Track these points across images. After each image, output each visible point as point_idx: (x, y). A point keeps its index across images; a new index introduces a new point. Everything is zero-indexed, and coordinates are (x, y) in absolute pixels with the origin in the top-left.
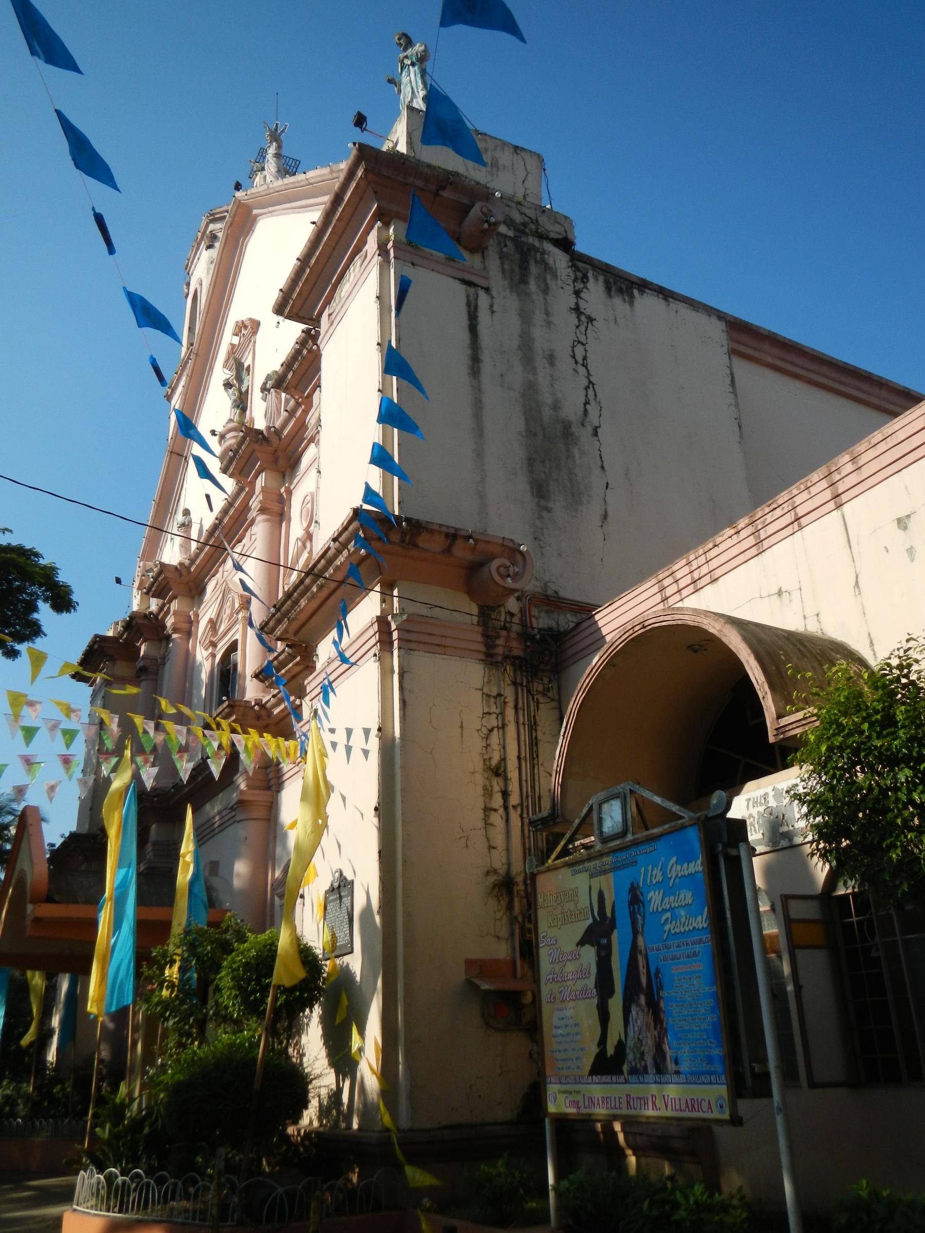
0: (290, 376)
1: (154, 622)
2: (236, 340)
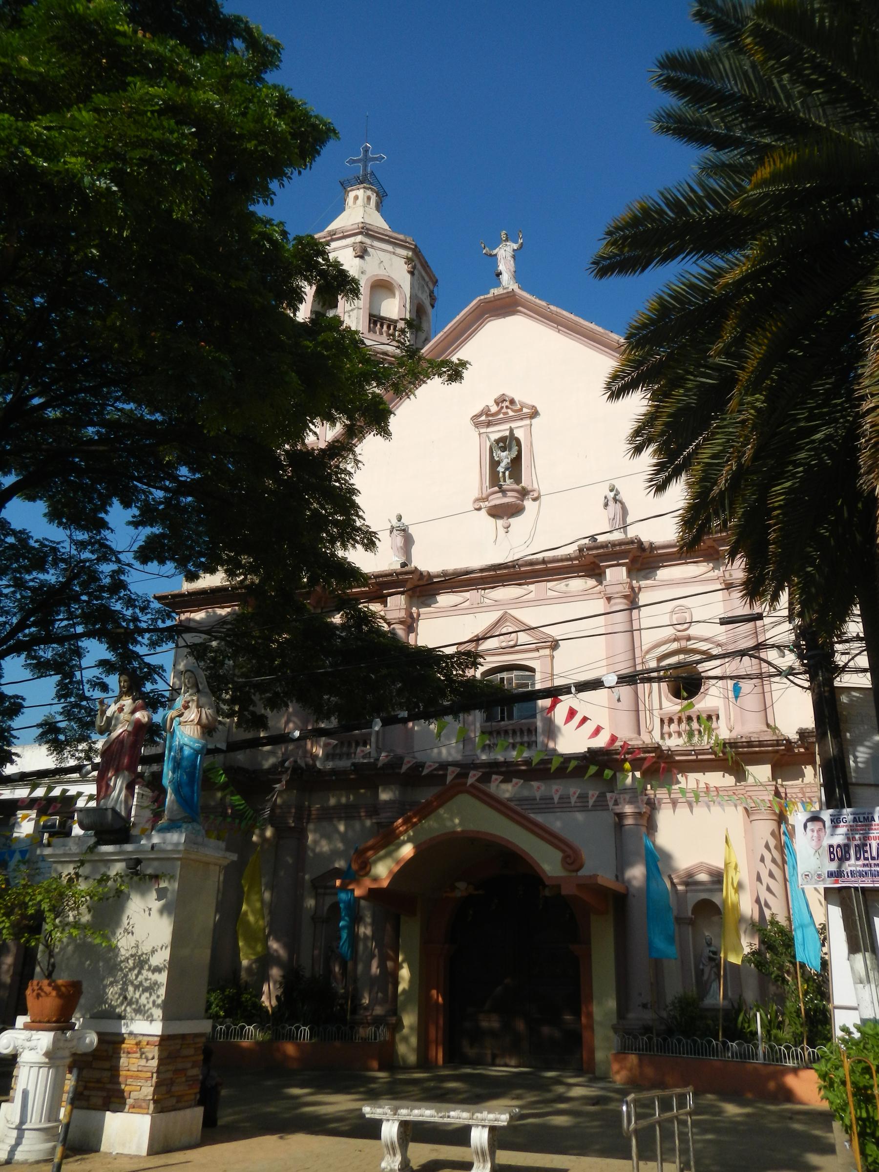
2: (494, 409)
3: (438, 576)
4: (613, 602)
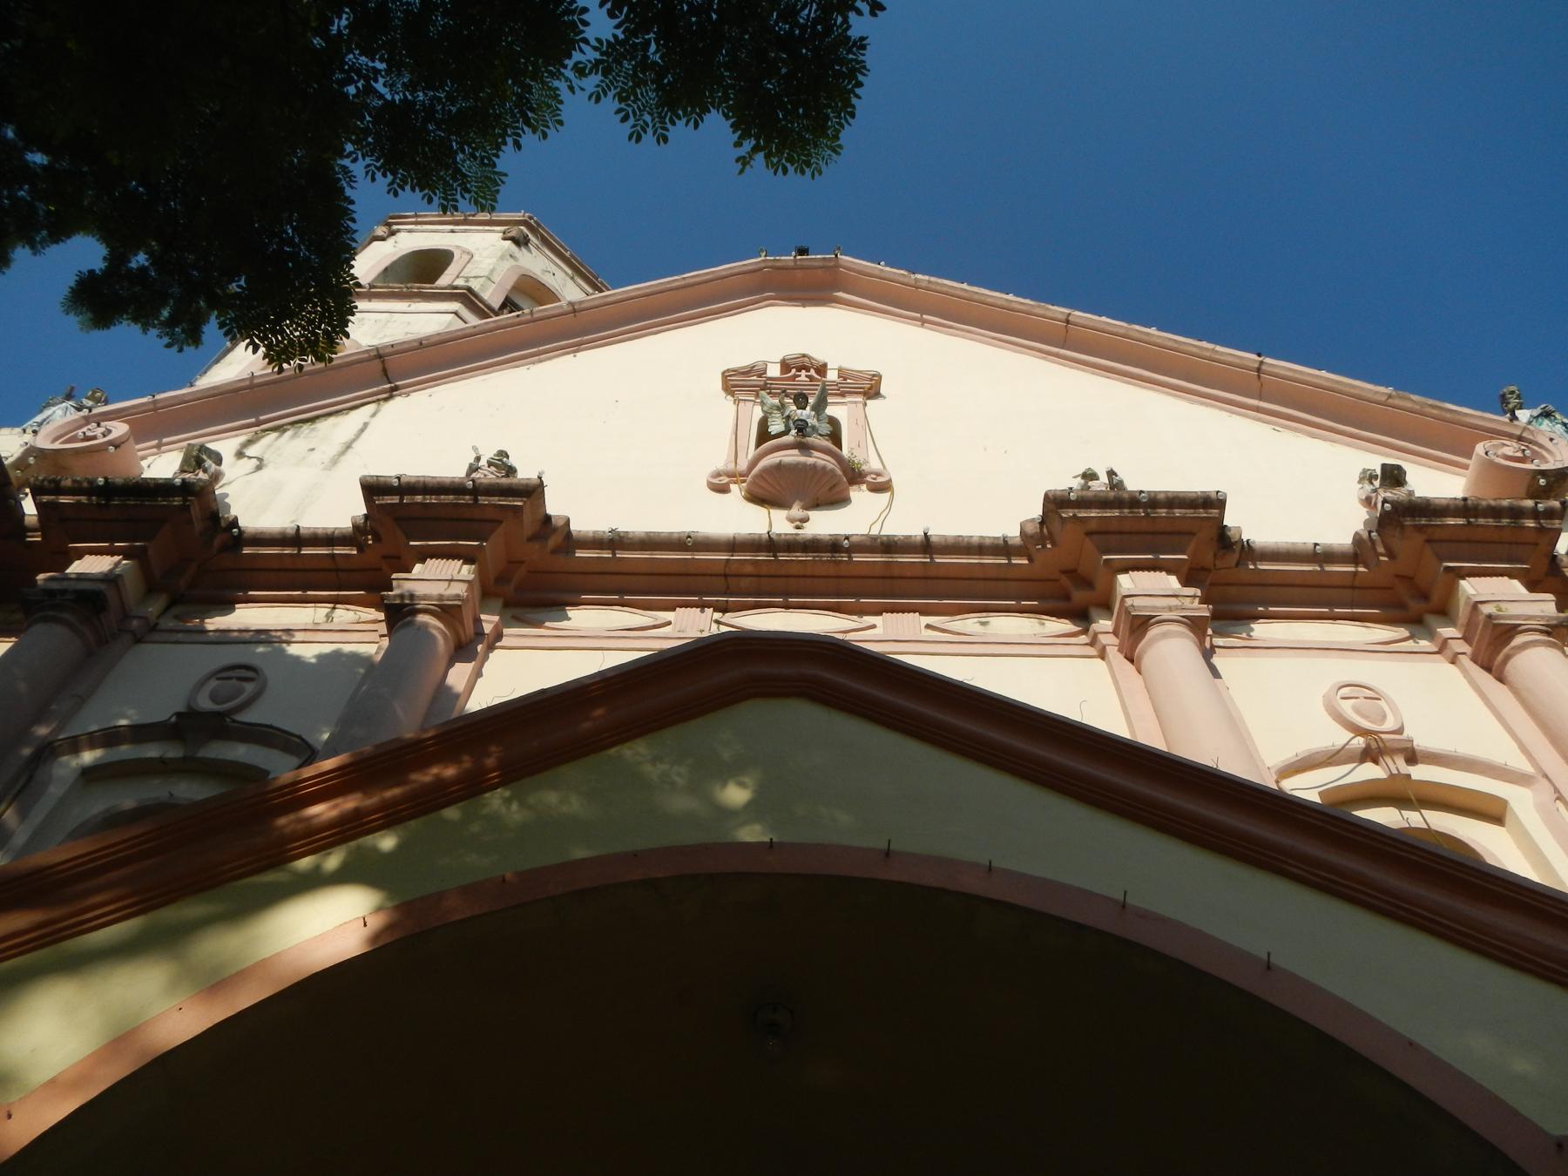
0: (1451, 521)
1: (217, 542)
3: (596, 542)
4: (1154, 632)
